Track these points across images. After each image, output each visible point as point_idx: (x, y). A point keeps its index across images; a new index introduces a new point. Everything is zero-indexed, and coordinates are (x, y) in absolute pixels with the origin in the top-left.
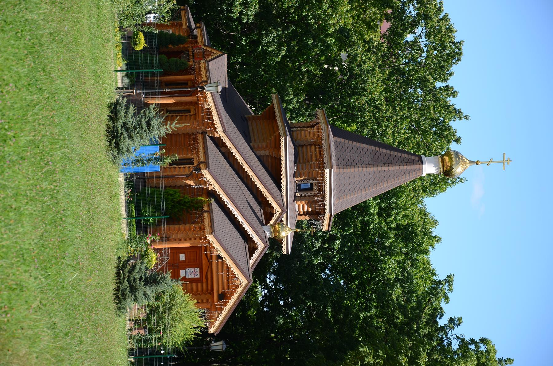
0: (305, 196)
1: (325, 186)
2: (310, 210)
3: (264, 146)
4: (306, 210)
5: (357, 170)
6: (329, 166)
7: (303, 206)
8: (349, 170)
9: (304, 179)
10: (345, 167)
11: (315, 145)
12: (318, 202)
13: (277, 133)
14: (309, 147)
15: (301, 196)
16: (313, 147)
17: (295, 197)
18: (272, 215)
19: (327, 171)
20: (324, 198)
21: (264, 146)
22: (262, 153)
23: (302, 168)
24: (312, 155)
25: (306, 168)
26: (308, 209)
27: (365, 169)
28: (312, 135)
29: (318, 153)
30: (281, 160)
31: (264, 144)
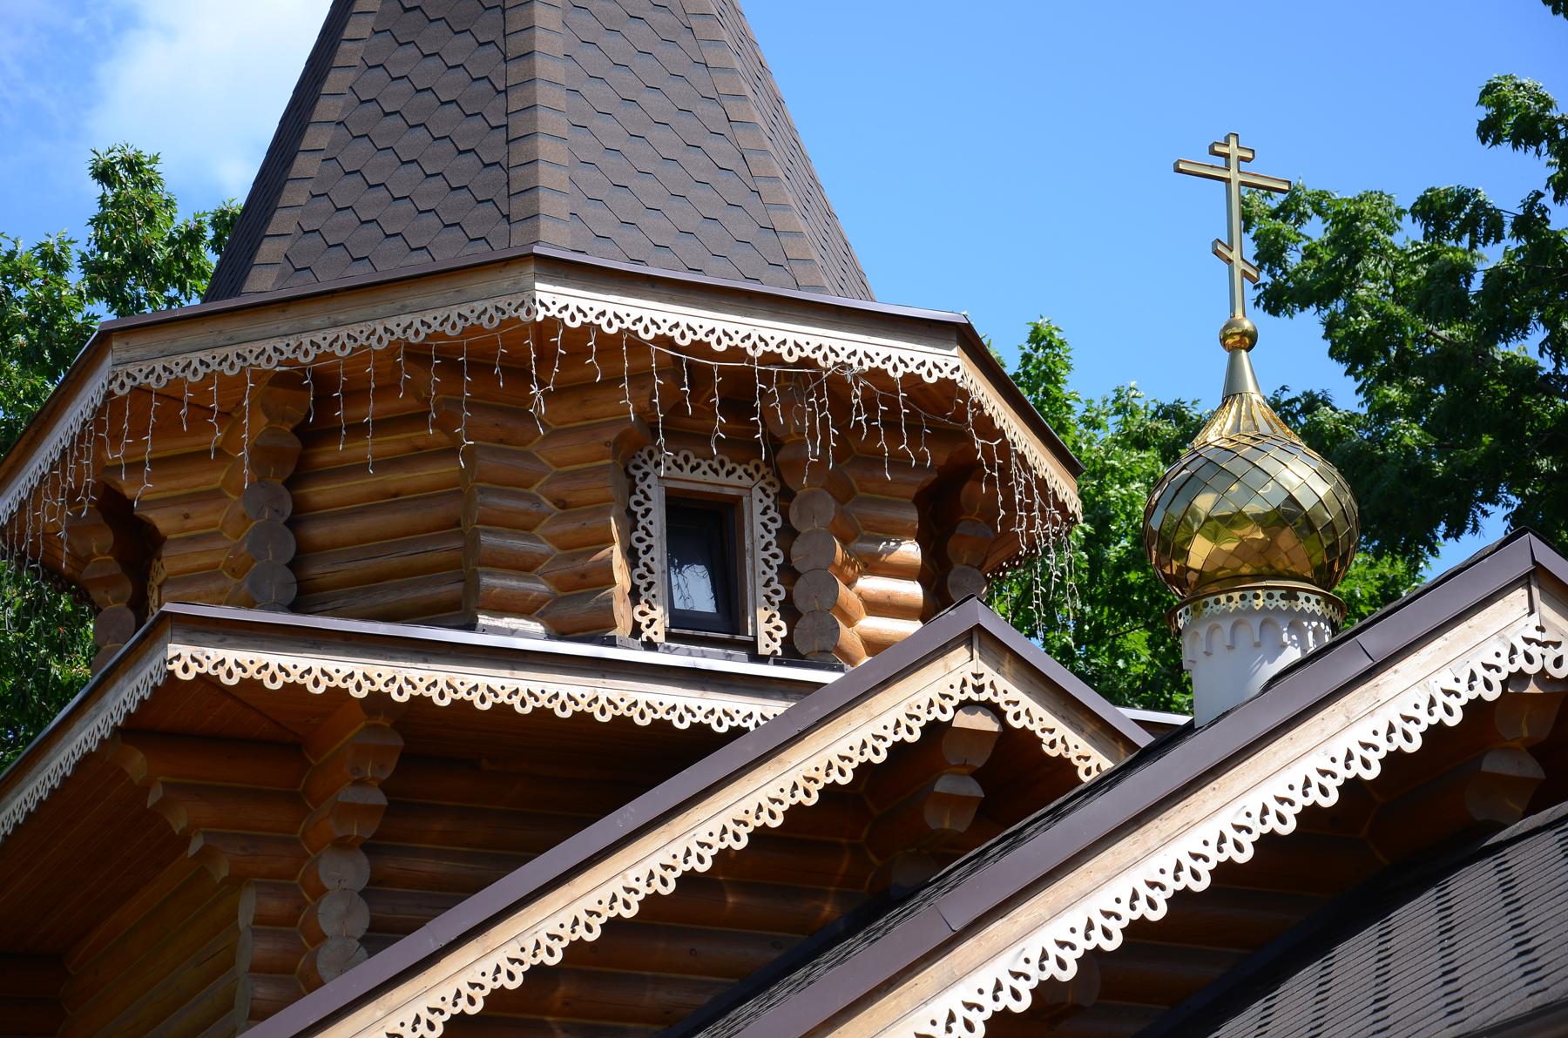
0: (789, 573)
1: (700, 348)
2: (910, 551)
3: (274, 906)
4: (912, 591)
5: (546, 121)
6: (504, 281)
7: (877, 607)
8: (547, 176)
9: (632, 556)
10: (517, 207)
11: (301, 475)
12: (848, 434)
13: (137, 764)
14: (319, 532)
15: (789, 611)
16: (322, 493)
17: (791, 654)
18: (1016, 746)
19: (557, 300)
20: (803, 377)
21: (274, 906)
22: (339, 917)
23: (523, 566)
24: (393, 499)
25: (524, 528)
26: (900, 572)
27: (544, 67)
28: (204, 516)
29: (368, 448)
30: (420, 703)
31: (248, 906)
